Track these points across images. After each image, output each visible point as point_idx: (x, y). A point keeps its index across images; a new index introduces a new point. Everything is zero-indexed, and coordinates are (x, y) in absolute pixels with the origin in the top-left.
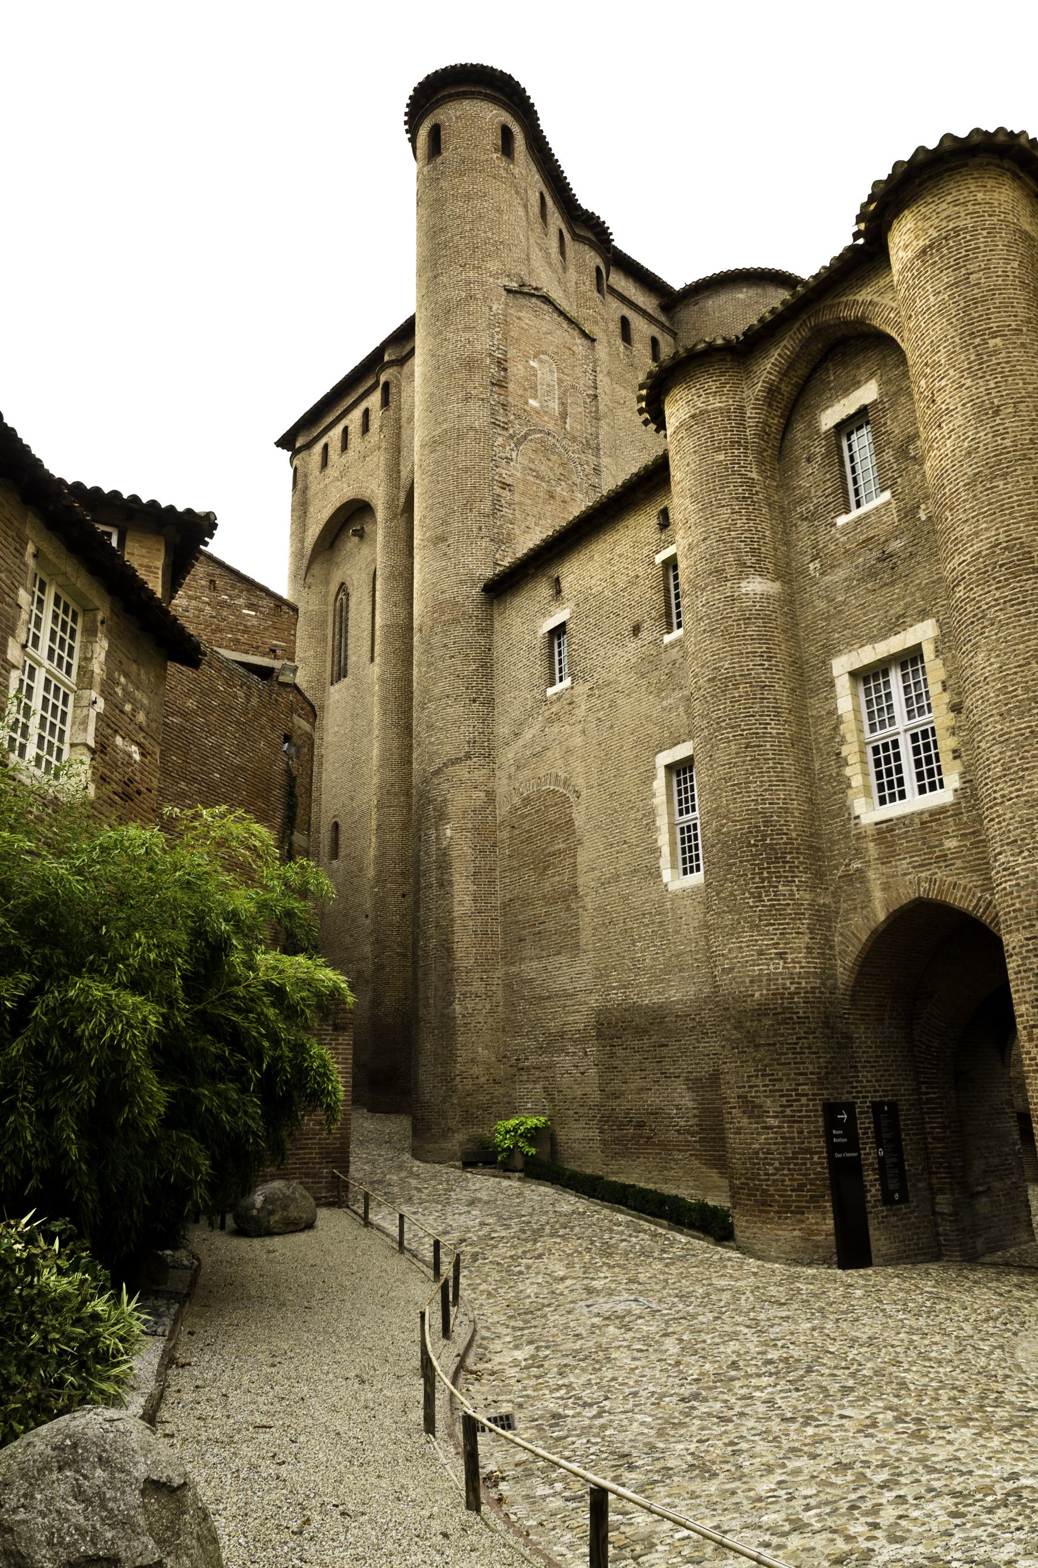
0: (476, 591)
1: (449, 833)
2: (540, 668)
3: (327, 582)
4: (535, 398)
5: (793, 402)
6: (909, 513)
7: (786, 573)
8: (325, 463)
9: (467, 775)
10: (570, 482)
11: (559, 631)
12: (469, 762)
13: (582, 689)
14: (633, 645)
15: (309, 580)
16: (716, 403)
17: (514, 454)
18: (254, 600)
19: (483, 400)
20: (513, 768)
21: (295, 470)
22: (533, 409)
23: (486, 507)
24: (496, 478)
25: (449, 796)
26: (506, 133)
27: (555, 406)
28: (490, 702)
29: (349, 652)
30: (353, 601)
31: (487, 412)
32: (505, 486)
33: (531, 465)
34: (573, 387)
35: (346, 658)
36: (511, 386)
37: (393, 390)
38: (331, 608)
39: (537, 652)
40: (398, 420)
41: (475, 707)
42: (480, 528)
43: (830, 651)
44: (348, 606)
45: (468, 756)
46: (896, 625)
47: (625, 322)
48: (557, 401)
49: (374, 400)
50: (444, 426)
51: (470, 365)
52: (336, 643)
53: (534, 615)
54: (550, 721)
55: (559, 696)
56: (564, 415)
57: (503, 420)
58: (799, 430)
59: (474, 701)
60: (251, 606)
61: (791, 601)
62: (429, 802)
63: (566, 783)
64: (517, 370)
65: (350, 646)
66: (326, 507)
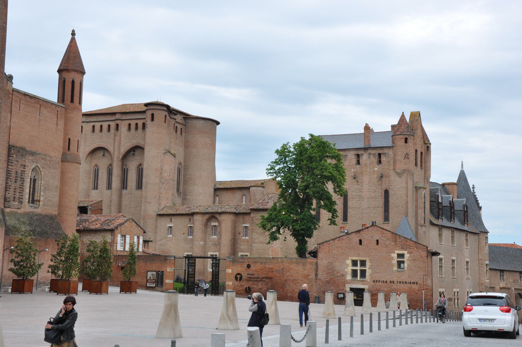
0: (155, 214)
2: (166, 231)
3: (91, 162)
5: (208, 220)
6: (218, 240)
7: (205, 241)
8: (93, 131)
11: (171, 227)
13: (173, 238)
14: (183, 236)
15: (87, 161)
16: (201, 219)
23: (158, 198)
26: (166, 116)
28: (156, 233)
30: (100, 172)
32: (161, 193)
36: (163, 173)
37: (119, 127)
38: (92, 169)
40: (120, 135)
43: (209, 251)
44: (98, 171)
46: (215, 252)
47: (176, 127)
49: (113, 124)
51: (157, 170)
53: (166, 223)
55: (170, 238)
58: (209, 223)
61: (205, 244)
64: (164, 169)
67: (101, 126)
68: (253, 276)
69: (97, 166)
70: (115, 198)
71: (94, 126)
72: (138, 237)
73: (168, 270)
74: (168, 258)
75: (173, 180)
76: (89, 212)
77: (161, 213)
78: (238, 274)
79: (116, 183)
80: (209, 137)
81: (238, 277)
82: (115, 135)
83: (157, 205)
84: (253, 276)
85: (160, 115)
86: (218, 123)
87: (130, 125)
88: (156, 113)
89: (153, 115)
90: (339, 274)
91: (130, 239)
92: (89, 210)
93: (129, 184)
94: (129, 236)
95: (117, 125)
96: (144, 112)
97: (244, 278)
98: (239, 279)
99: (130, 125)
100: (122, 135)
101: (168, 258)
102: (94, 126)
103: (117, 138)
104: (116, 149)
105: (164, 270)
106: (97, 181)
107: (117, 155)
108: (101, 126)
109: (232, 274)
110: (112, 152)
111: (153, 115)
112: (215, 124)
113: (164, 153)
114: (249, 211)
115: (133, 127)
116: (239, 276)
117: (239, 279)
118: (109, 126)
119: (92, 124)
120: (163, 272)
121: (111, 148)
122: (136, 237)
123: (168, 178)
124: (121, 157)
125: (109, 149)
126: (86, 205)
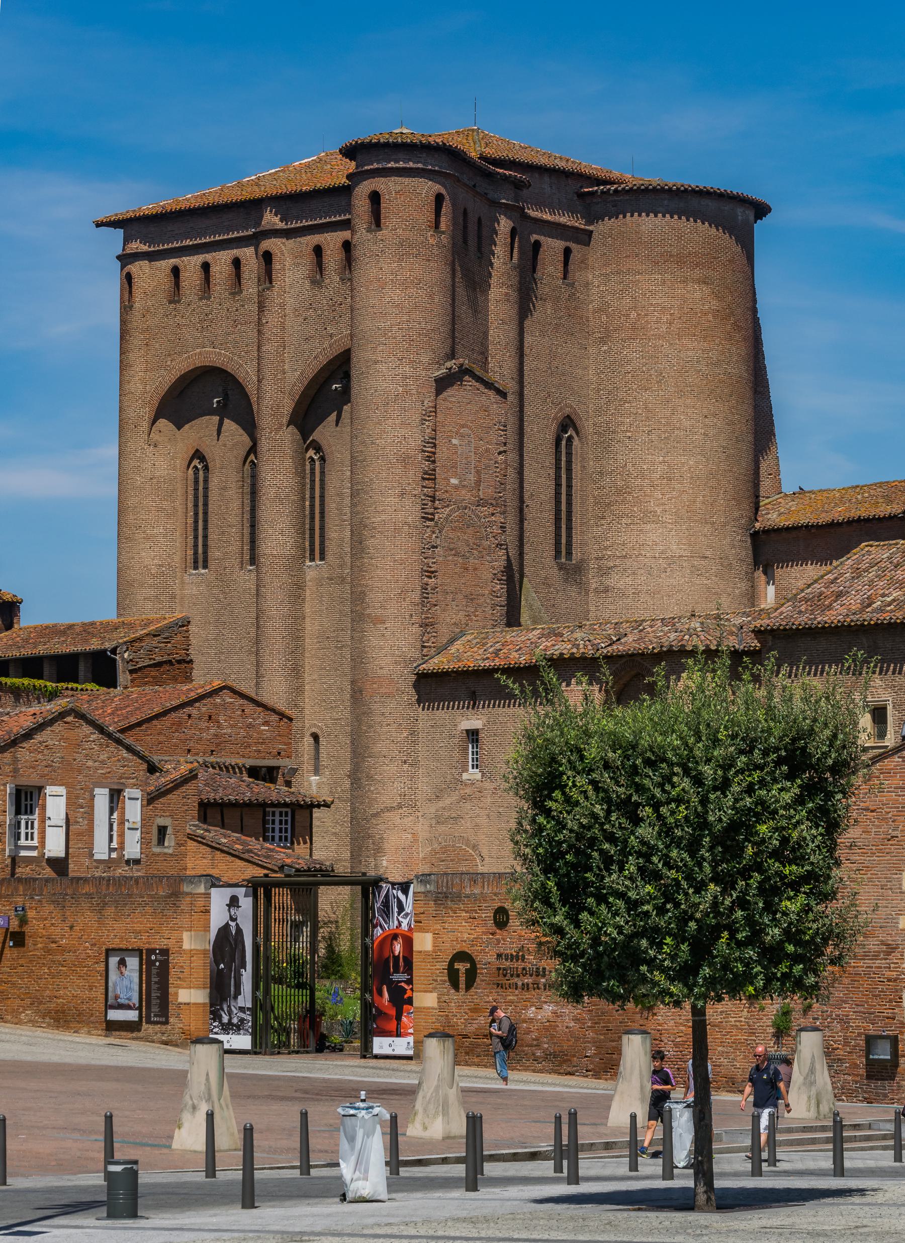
1: (385, 863)
2: (456, 754)
4: (455, 475)
9: (399, 821)
10: (480, 549)
11: (473, 735)
12: (400, 811)
13: (488, 785)
17: (438, 540)
18: (267, 719)
19: (415, 496)
20: (434, 822)
21: (129, 278)
22: (456, 487)
23: (416, 596)
24: (425, 568)
25: (385, 836)
26: (439, 199)
27: (472, 477)
29: (210, 543)
31: (419, 507)
33: (452, 546)
34: (487, 450)
35: (205, 546)
37: (276, 266)
39: (456, 741)
40: (282, 306)
41: (406, 767)
42: (411, 615)
44: (206, 481)
45: (400, 806)
48: (473, 471)
50: (383, 517)
52: (190, 521)
54: (464, 798)
56: (478, 483)
57: (431, 510)
59: (405, 762)
60: (266, 723)
62: (369, 837)
63: (474, 847)
65: (212, 536)
66: (180, 354)
67: (206, 266)
68: (520, 965)
69: (202, 459)
70: (276, 604)
71: (176, 271)
72: (116, 796)
73: (186, 946)
74: (186, 888)
75: (496, 503)
76: (123, 677)
77: (438, 663)
78: (461, 956)
79: (279, 535)
80: (704, 281)
81: (462, 971)
82: (261, 307)
83: (416, 629)
84: (520, 965)
85: (409, 197)
86: (761, 210)
87: (318, 250)
88: (387, 186)
89: (375, 198)
90: (872, 945)
91: (71, 803)
92: (120, 665)
93: (332, 534)
94: (62, 790)
95: (268, 257)
96: (343, 192)
97: (483, 972)
98: (462, 979)
99: (318, 250)
100: (290, 302)
101: (186, 888)
102: (176, 271)
103: (272, 319)
104: (267, 373)
105: (170, 944)
106: (205, 528)
107: (275, 400)
108: (206, 266)
109: (433, 956)
110: (251, 389)
111: (375, 198)
112: (743, 214)
113: (438, 381)
114: (756, 644)
115: (333, 257)
116: (461, 967)
117: (462, 979)
118: (237, 263)
119: (166, 264)
120: (165, 952)
121: (246, 373)
122: (102, 798)
123: (466, 496)
124: (287, 407)
125: (240, 376)
126: (108, 645)
